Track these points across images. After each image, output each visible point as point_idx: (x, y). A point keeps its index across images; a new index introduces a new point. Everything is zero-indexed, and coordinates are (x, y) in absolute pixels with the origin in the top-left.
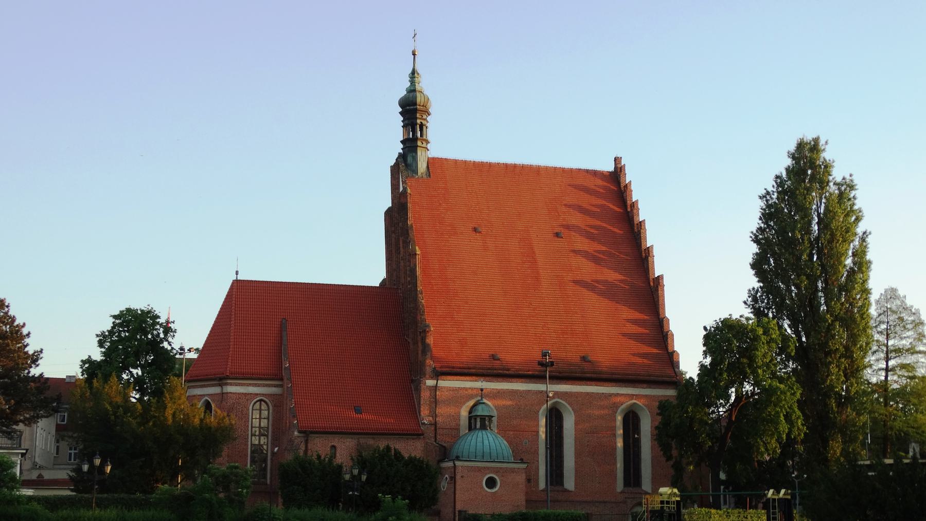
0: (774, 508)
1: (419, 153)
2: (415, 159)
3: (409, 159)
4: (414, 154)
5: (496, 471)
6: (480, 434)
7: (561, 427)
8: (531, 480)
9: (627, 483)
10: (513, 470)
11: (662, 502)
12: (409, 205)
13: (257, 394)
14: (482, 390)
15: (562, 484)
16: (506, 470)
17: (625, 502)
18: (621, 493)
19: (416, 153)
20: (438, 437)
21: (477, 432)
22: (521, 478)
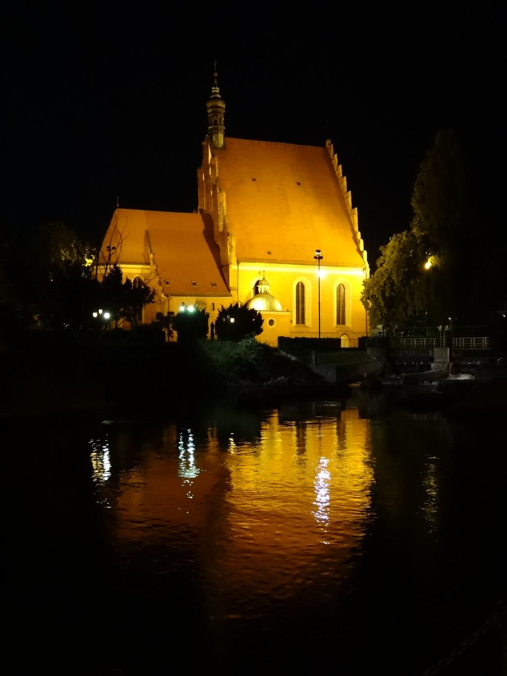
0: (442, 335)
1: (219, 135)
2: (217, 138)
3: (214, 138)
5: (275, 316)
6: (264, 295)
8: (291, 322)
9: (338, 322)
10: (283, 316)
12: (217, 166)
13: (135, 274)
14: (264, 271)
16: (279, 316)
17: (337, 333)
18: (336, 327)
19: (218, 135)
20: (239, 297)
22: (288, 320)
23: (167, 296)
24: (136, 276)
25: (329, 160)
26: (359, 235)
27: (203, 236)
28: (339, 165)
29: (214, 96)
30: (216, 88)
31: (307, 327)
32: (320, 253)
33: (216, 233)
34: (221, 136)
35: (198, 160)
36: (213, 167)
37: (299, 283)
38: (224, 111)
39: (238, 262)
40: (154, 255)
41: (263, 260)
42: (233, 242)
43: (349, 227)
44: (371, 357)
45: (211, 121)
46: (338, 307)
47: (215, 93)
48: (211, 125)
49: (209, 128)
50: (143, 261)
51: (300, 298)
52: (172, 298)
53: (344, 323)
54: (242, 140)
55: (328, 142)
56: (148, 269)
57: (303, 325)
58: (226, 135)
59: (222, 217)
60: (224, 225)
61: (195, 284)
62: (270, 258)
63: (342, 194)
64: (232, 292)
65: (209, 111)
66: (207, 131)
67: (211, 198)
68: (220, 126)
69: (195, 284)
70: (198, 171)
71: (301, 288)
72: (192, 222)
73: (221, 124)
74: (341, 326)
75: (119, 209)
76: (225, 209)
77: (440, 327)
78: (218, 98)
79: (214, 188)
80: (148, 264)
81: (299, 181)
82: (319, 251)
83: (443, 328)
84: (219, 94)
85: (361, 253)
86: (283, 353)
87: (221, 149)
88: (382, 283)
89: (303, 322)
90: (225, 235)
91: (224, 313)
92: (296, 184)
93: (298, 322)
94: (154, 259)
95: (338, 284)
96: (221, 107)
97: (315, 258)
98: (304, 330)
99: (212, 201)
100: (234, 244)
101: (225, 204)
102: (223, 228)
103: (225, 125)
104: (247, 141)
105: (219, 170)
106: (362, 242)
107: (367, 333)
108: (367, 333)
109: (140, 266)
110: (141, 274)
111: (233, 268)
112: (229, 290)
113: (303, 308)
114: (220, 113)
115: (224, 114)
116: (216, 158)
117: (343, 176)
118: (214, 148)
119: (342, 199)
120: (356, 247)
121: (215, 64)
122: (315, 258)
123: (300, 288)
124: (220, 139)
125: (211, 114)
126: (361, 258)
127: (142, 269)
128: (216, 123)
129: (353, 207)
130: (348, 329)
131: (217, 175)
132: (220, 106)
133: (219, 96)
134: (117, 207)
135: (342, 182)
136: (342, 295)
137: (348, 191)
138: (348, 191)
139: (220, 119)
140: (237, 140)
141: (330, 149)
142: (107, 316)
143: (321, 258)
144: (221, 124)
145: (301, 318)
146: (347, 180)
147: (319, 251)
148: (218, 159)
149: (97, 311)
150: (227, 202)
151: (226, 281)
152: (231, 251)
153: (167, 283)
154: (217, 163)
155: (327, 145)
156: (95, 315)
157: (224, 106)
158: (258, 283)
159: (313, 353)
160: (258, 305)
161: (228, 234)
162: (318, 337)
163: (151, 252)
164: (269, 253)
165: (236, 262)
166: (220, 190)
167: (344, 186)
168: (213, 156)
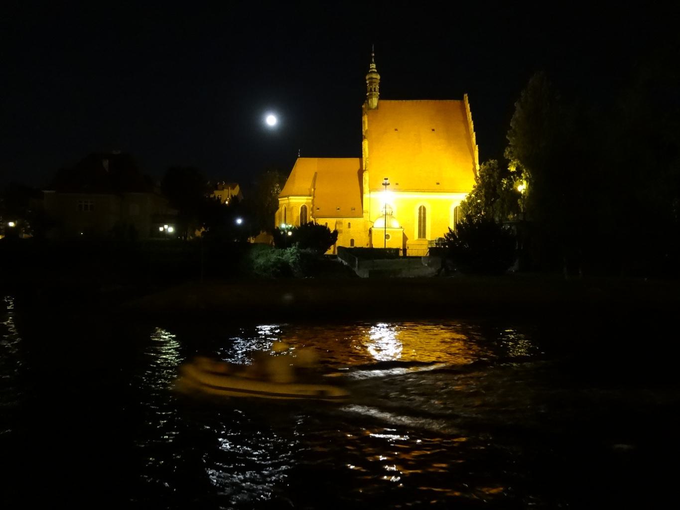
1: (374, 99)
2: (372, 102)
7: (424, 214)
13: (303, 203)
23: (314, 218)
24: (303, 204)
27: (357, 174)
29: (371, 70)
32: (387, 181)
37: (421, 207)
38: (379, 81)
39: (370, 191)
40: (315, 189)
42: (366, 176)
43: (472, 161)
44: (424, 264)
47: (372, 68)
50: (308, 194)
54: (393, 101)
55: (466, 95)
56: (310, 199)
57: (424, 239)
58: (381, 98)
61: (338, 209)
64: (364, 214)
65: (368, 82)
68: (374, 92)
69: (338, 209)
71: (422, 212)
75: (300, 158)
78: (374, 72)
80: (310, 196)
86: (340, 259)
89: (424, 236)
92: (431, 130)
93: (420, 236)
95: (456, 206)
96: (376, 79)
97: (383, 184)
103: (380, 91)
104: (396, 101)
105: (368, 124)
109: (306, 198)
110: (306, 203)
111: (366, 196)
115: (379, 83)
119: (469, 138)
122: (383, 184)
123: (422, 211)
124: (374, 102)
127: (307, 199)
128: (371, 90)
132: (375, 77)
133: (376, 71)
134: (298, 157)
139: (375, 88)
140: (388, 101)
142: (171, 230)
143: (385, 184)
144: (375, 91)
146: (474, 124)
149: (163, 227)
152: (365, 184)
153: (318, 209)
156: (161, 229)
157: (378, 77)
159: (357, 259)
160: (378, 225)
162: (384, 247)
165: (368, 192)
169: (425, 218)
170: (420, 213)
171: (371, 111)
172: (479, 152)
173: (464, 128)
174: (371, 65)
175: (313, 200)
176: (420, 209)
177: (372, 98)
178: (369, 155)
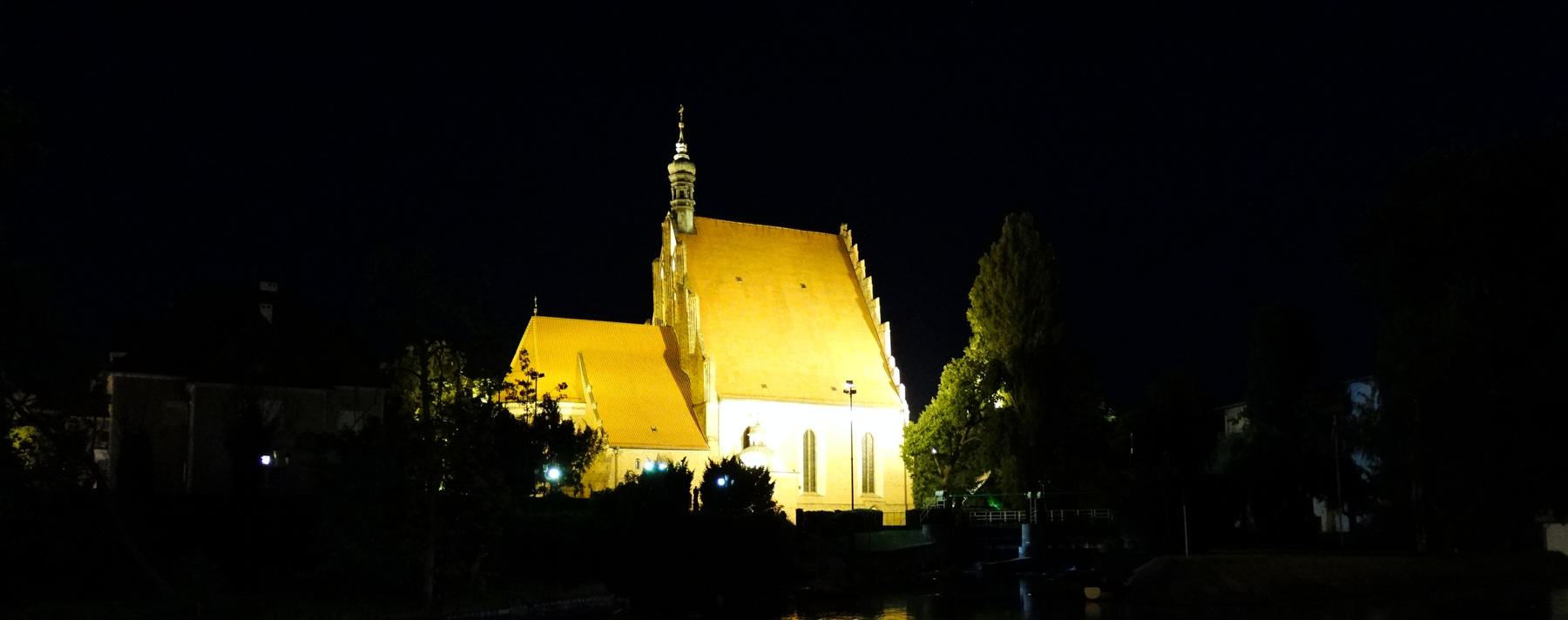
4: (683, 213)
7: (813, 445)
9: (865, 490)
11: (940, 503)
12: (685, 257)
15: (814, 490)
19: (685, 213)
21: (756, 448)
23: (615, 448)
25: (846, 253)
26: (892, 361)
28: (860, 260)
30: (683, 145)
31: (819, 496)
33: (683, 356)
34: (690, 215)
35: (654, 247)
36: (679, 259)
38: (694, 179)
41: (755, 396)
42: (712, 369)
43: (879, 350)
45: (675, 192)
46: (865, 466)
48: (675, 198)
49: (672, 203)
51: (809, 453)
52: (622, 452)
53: (872, 490)
54: (720, 222)
55: (844, 227)
57: (813, 493)
58: (696, 214)
59: (694, 333)
60: (697, 345)
62: (763, 392)
63: (865, 301)
64: (710, 444)
65: (672, 178)
66: (668, 207)
67: (674, 306)
68: (688, 200)
70: (655, 265)
71: (810, 441)
72: (643, 338)
73: (689, 198)
74: (869, 494)
76: (699, 320)
77: (1029, 494)
79: (681, 289)
81: (803, 283)
82: (851, 382)
83: (1034, 495)
84: (686, 153)
85: (895, 388)
87: (690, 233)
88: (934, 431)
89: (814, 490)
90: (698, 359)
91: (713, 472)
92: (800, 287)
93: (806, 489)
94: (591, 395)
97: (846, 392)
98: (816, 500)
99: (676, 310)
100: (713, 371)
101: (698, 314)
102: (696, 350)
106: (897, 372)
107: (907, 505)
108: (907, 505)
111: (711, 409)
112: (706, 441)
113: (814, 469)
114: (689, 181)
115: (694, 183)
116: (684, 246)
117: (867, 276)
118: (680, 232)
120: (889, 380)
121: (681, 111)
122: (846, 392)
125: (676, 183)
126: (895, 393)
127: (573, 408)
128: (682, 196)
129: (883, 321)
130: (878, 500)
131: (685, 271)
133: (687, 157)
135: (866, 285)
136: (869, 450)
137: (875, 297)
138: (875, 297)
139: (689, 191)
140: (712, 221)
141: (846, 237)
143: (853, 392)
144: (689, 198)
145: (810, 484)
147: (851, 382)
148: (687, 247)
150: (702, 309)
151: (701, 426)
152: (709, 381)
154: (685, 253)
155: (842, 230)
157: (693, 171)
158: (748, 431)
161: (704, 358)
162: (851, 509)
163: (587, 382)
164: (764, 386)
166: (689, 292)
167: (869, 291)
168: (679, 243)
169: (814, 452)
170: (806, 444)
171: (683, 237)
172: (891, 333)
173: (854, 288)
174: (678, 145)
175: (596, 411)
176: (806, 434)
177: (684, 210)
178: (701, 323)
